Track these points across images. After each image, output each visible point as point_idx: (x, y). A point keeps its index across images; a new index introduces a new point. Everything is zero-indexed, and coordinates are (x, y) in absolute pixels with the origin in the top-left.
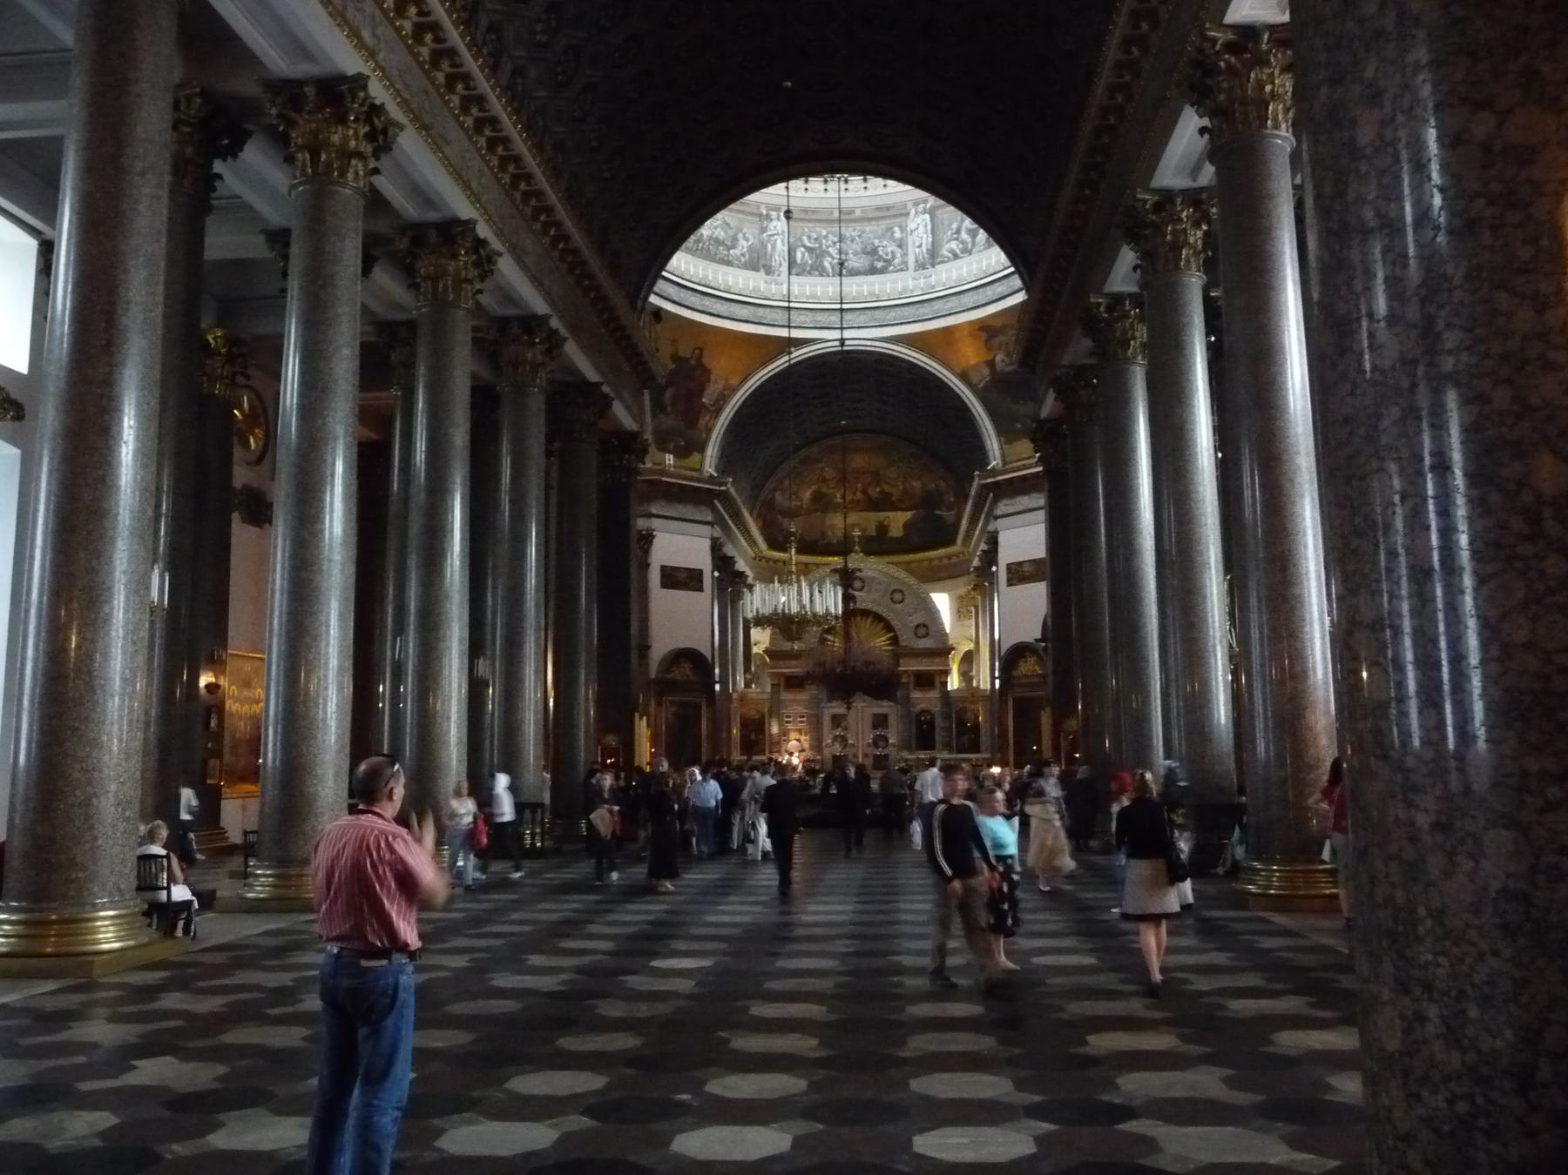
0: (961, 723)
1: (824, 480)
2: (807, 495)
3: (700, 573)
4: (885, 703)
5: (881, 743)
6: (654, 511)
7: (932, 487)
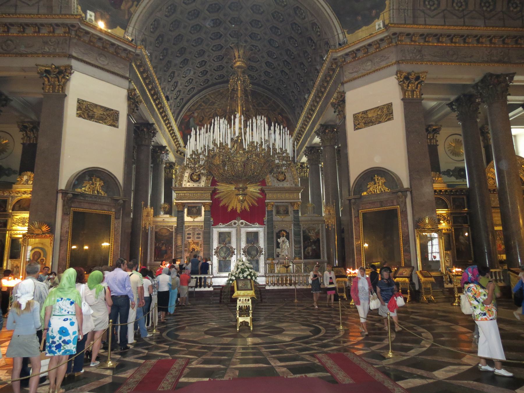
0: (306, 238)
5: (254, 253)
6: (74, 54)
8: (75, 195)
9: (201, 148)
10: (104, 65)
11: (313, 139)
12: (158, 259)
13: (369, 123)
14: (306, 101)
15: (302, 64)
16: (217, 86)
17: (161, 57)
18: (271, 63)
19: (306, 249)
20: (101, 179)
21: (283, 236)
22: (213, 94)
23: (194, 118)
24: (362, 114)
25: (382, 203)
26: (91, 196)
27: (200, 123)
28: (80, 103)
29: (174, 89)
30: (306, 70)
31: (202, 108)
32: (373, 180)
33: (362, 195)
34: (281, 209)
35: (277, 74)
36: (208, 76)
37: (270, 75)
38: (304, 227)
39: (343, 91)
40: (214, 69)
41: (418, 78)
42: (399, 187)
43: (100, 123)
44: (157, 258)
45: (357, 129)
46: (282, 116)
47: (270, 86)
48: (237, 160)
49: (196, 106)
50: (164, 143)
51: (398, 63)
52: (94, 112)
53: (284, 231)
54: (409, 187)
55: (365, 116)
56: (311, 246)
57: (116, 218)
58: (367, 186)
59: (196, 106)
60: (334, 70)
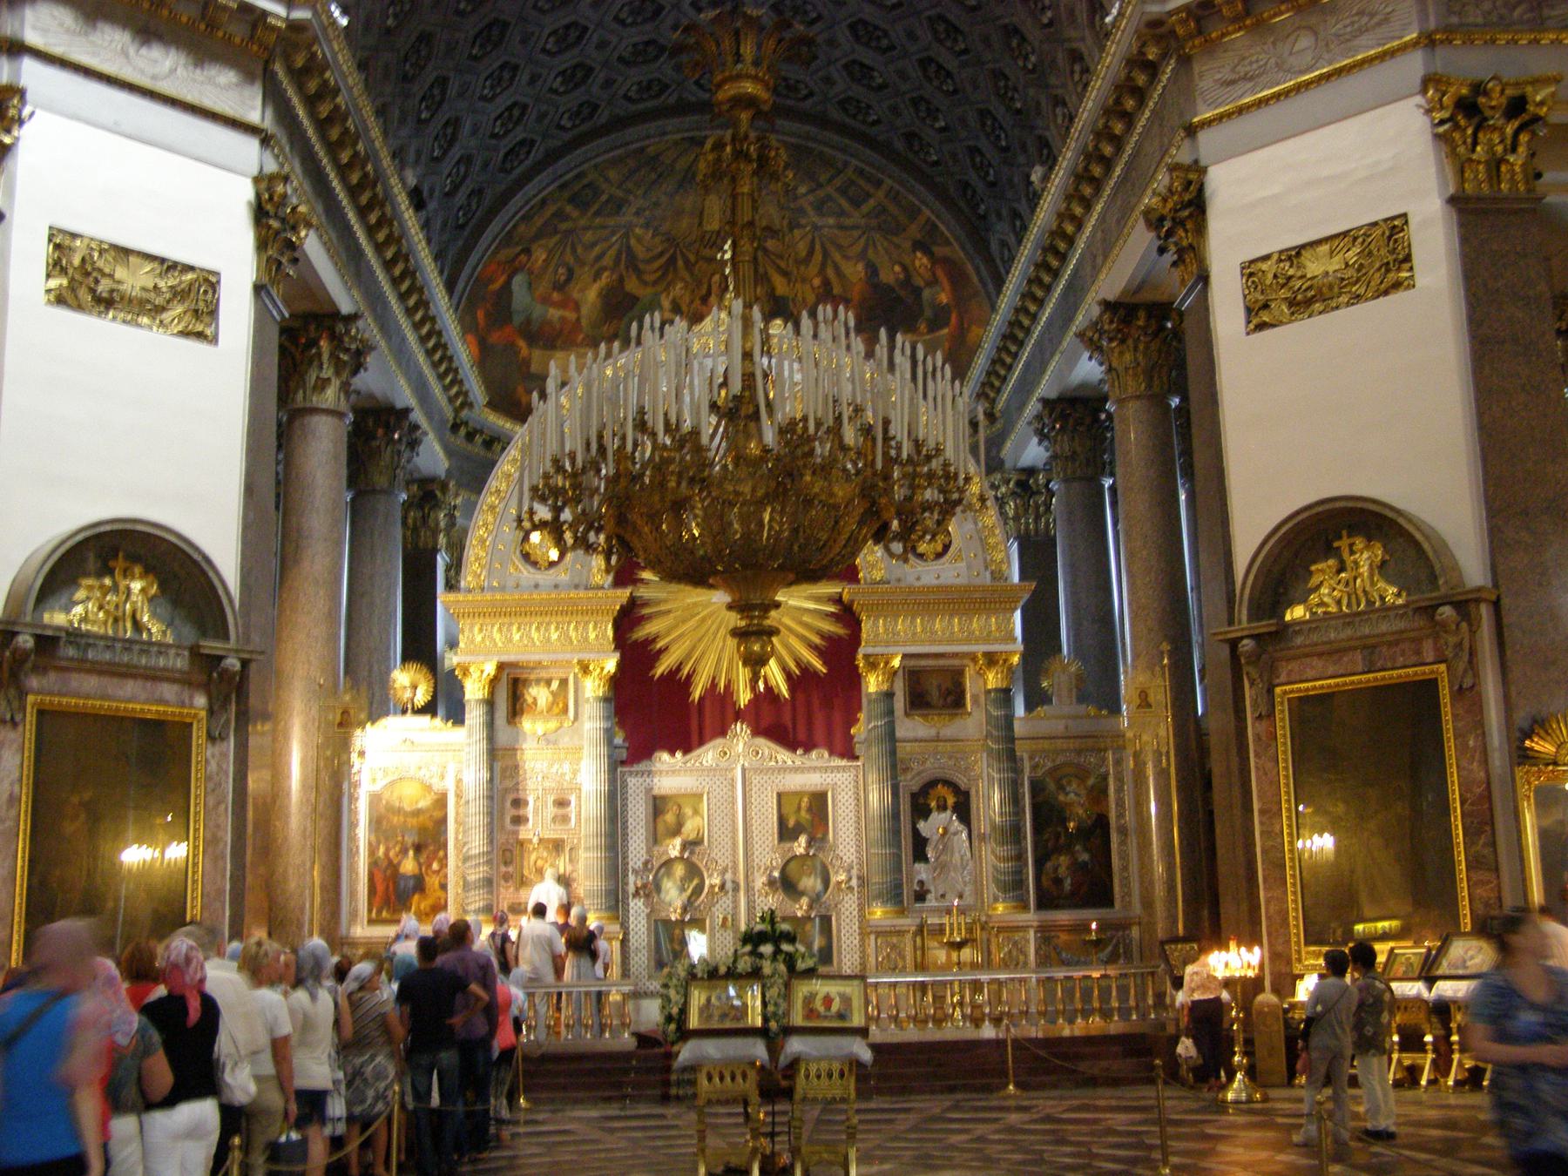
1: (633, 264)
2: (590, 296)
3: (209, 282)
4: (819, 757)
5: (810, 883)
7: (890, 274)
8: (47, 643)
9: (588, 444)
10: (154, 77)
11: (1072, 361)
12: (384, 914)
13: (1309, 302)
14: (1034, 199)
15: (1013, 31)
16: (632, 132)
17: (390, 22)
18: (876, 28)
19: (1049, 865)
20: (148, 570)
21: (942, 807)
22: (614, 163)
23: (531, 273)
24: (1281, 260)
25: (1371, 651)
26: (110, 642)
27: (556, 296)
28: (61, 243)
29: (445, 152)
30: (1033, 58)
31: (564, 226)
32: (1329, 551)
33: (1288, 617)
34: (933, 687)
35: (903, 75)
36: (595, 90)
37: (872, 78)
38: (1034, 768)
39: (1196, 162)
40: (621, 59)
41: (1517, 106)
42: (1441, 582)
43: (139, 325)
44: (379, 912)
45: (1261, 326)
46: (927, 251)
47: (875, 123)
48: (737, 493)
49: (538, 222)
50: (405, 396)
51: (1428, 41)
52: (119, 282)
53: (948, 783)
54: (1490, 585)
55: (1291, 272)
56: (1068, 849)
57: (211, 738)
58: (1306, 581)
59: (538, 222)
60: (1153, 69)
